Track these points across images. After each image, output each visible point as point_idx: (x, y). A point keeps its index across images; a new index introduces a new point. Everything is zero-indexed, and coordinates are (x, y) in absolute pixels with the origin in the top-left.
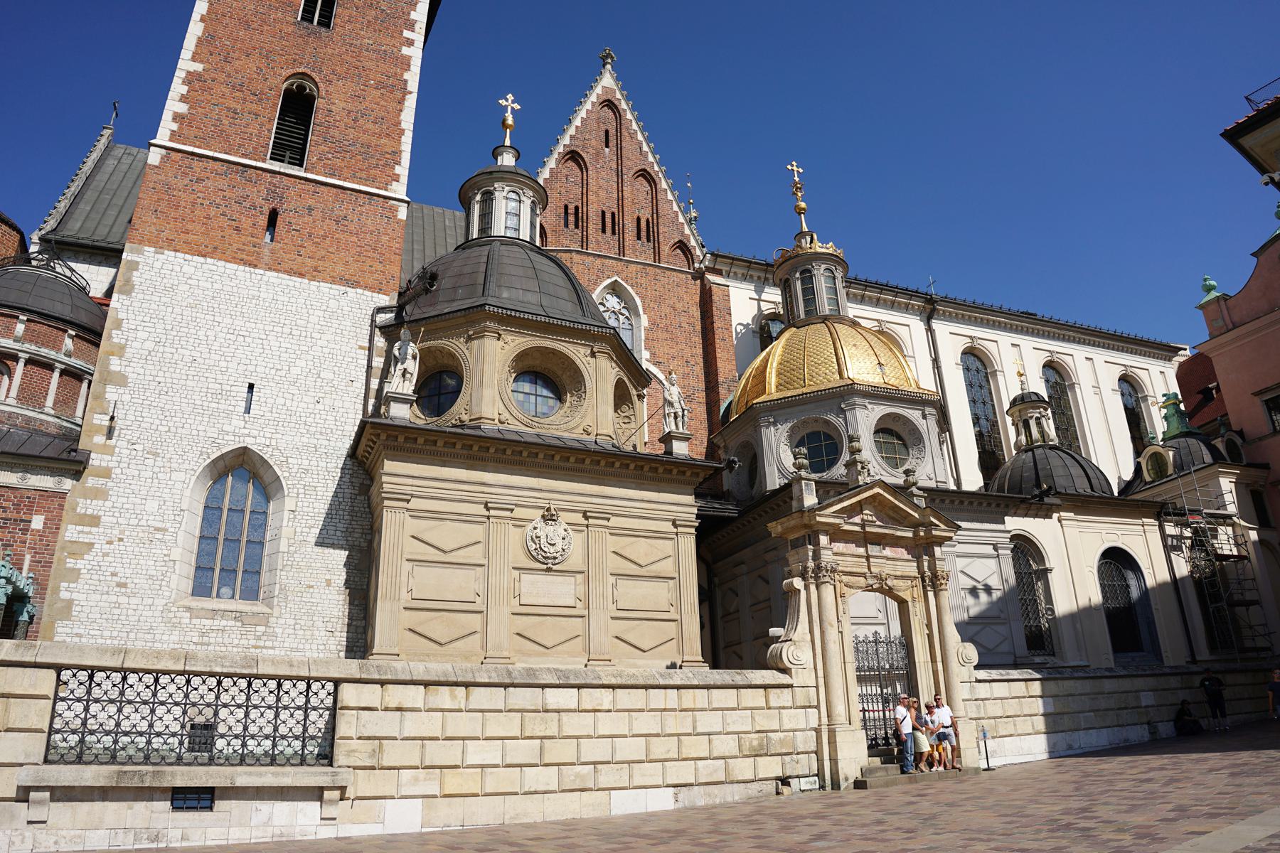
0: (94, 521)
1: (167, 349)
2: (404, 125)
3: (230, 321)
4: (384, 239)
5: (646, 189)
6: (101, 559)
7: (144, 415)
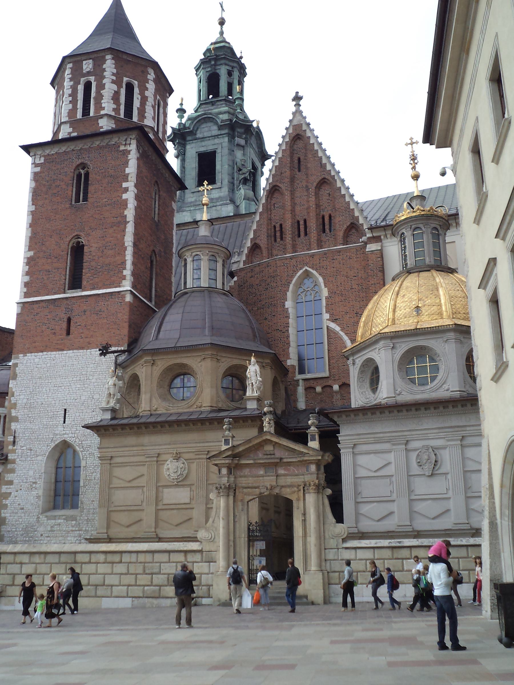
0: (11, 483)
1: (32, 401)
2: (126, 244)
3: (54, 380)
4: (120, 315)
5: (328, 192)
6: (14, 498)
7: (26, 433)
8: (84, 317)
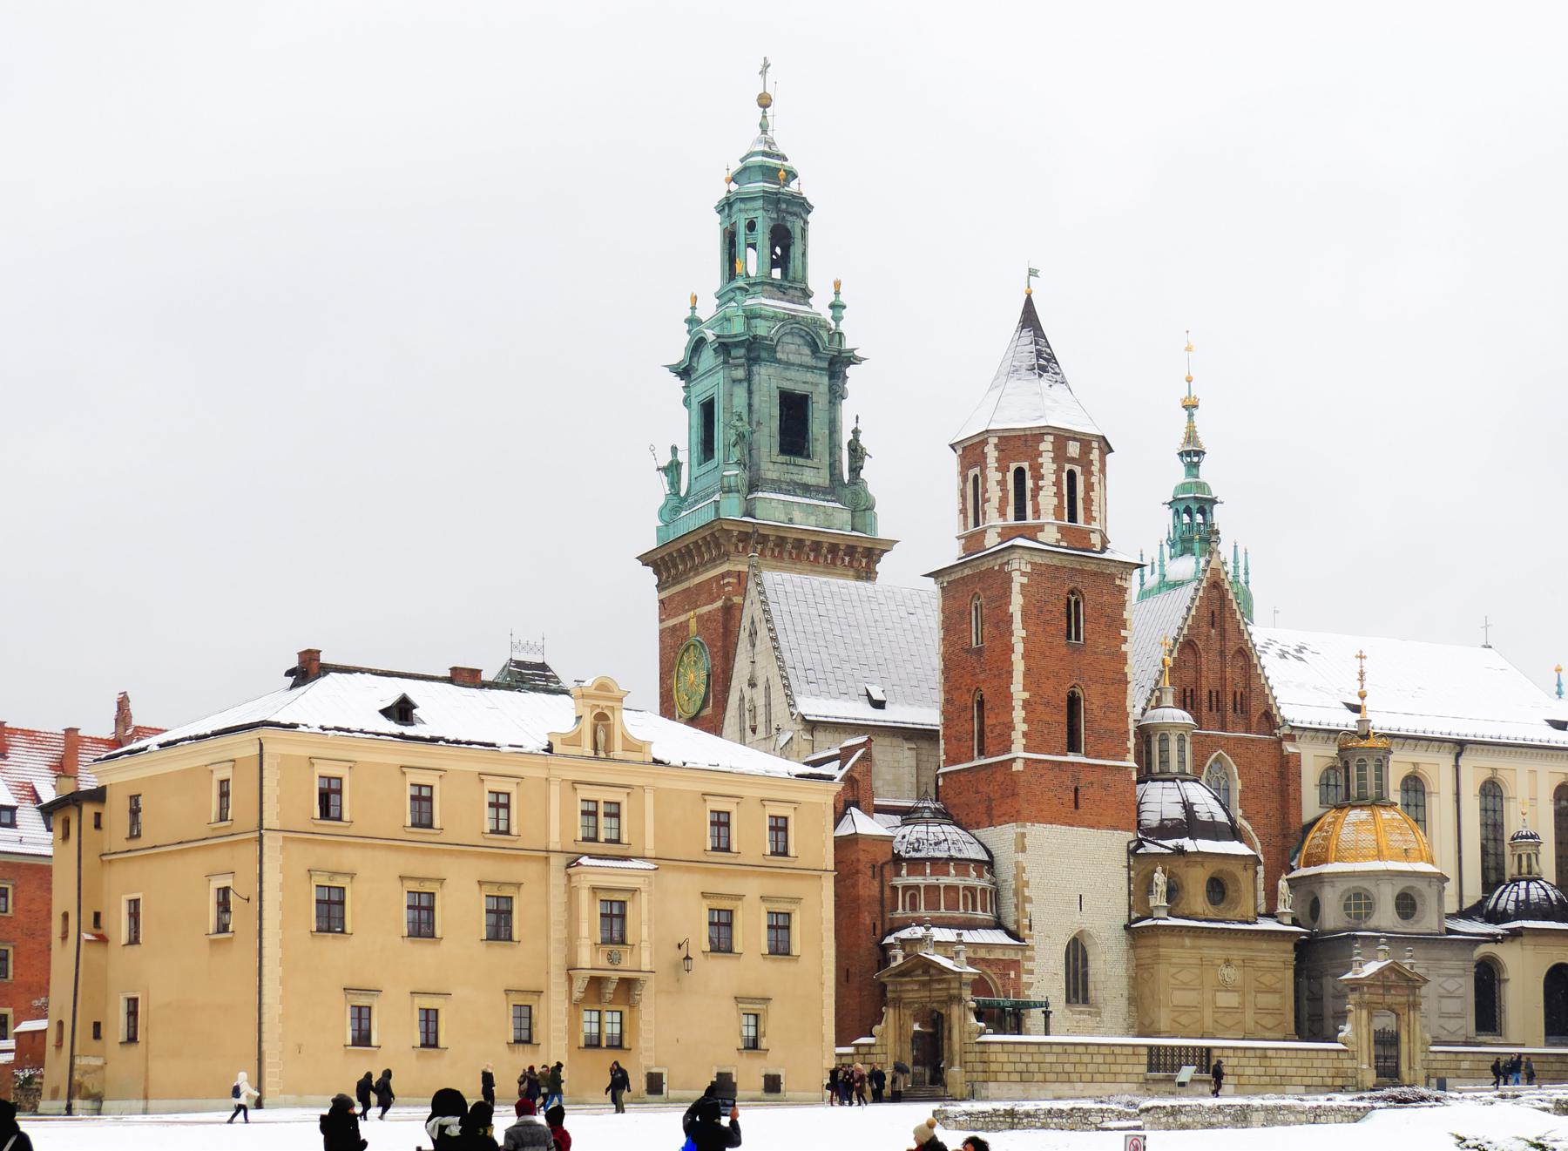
0: (1031, 972)
8: (1091, 790)
